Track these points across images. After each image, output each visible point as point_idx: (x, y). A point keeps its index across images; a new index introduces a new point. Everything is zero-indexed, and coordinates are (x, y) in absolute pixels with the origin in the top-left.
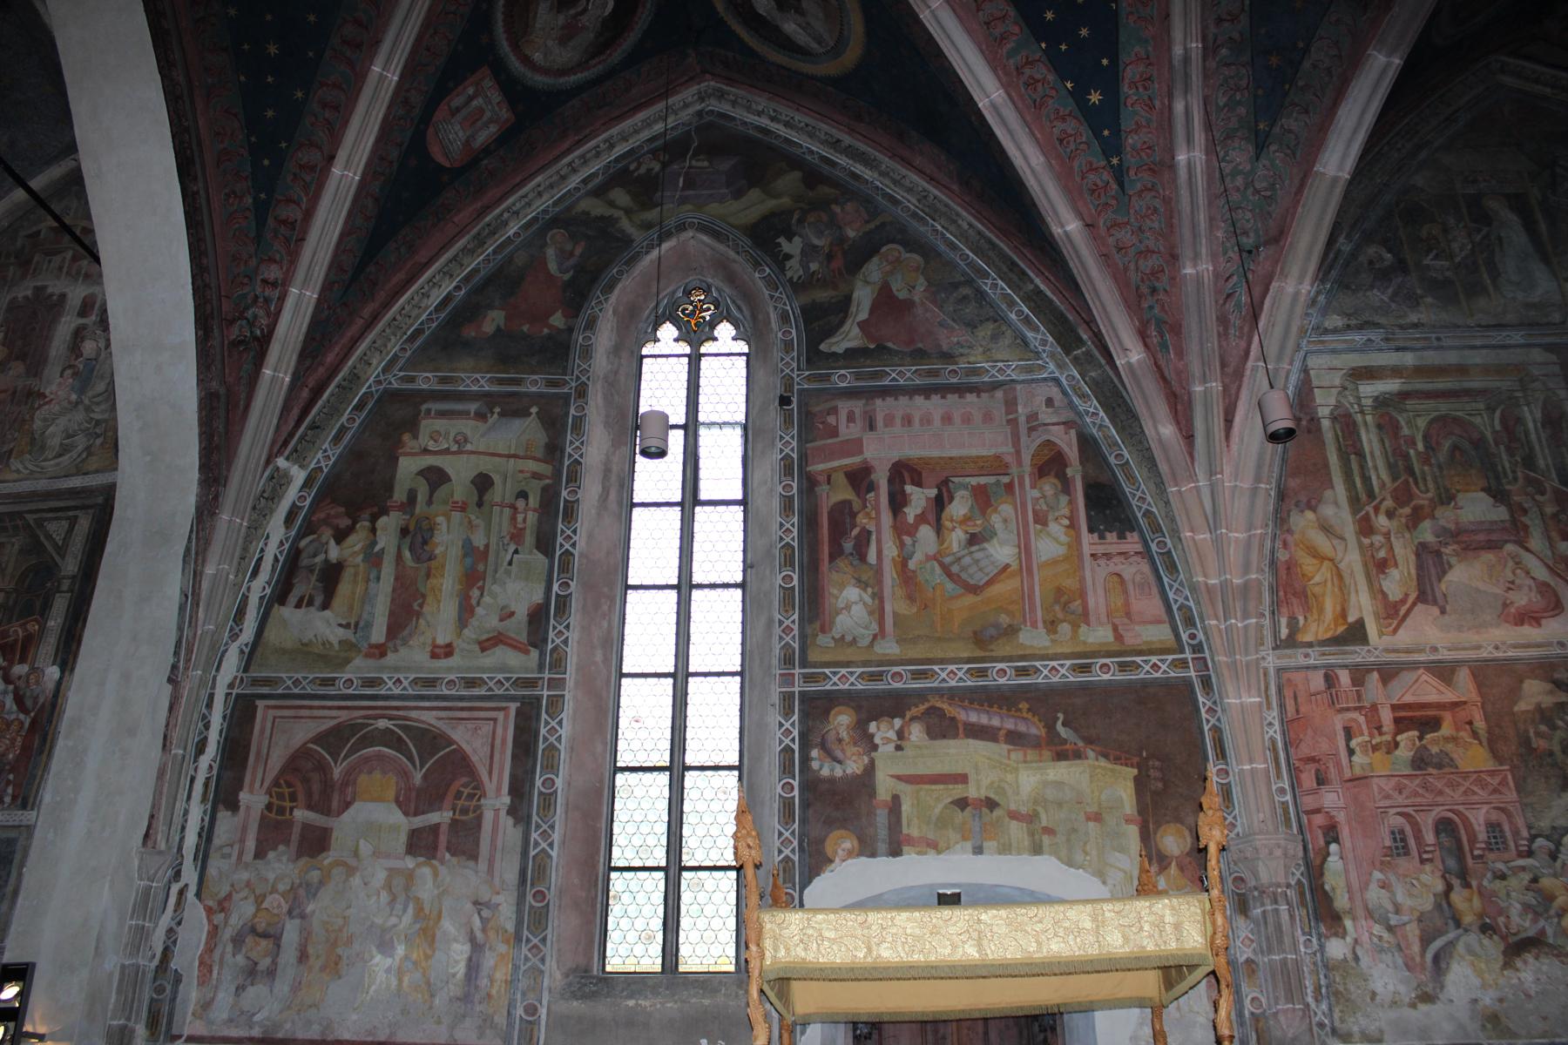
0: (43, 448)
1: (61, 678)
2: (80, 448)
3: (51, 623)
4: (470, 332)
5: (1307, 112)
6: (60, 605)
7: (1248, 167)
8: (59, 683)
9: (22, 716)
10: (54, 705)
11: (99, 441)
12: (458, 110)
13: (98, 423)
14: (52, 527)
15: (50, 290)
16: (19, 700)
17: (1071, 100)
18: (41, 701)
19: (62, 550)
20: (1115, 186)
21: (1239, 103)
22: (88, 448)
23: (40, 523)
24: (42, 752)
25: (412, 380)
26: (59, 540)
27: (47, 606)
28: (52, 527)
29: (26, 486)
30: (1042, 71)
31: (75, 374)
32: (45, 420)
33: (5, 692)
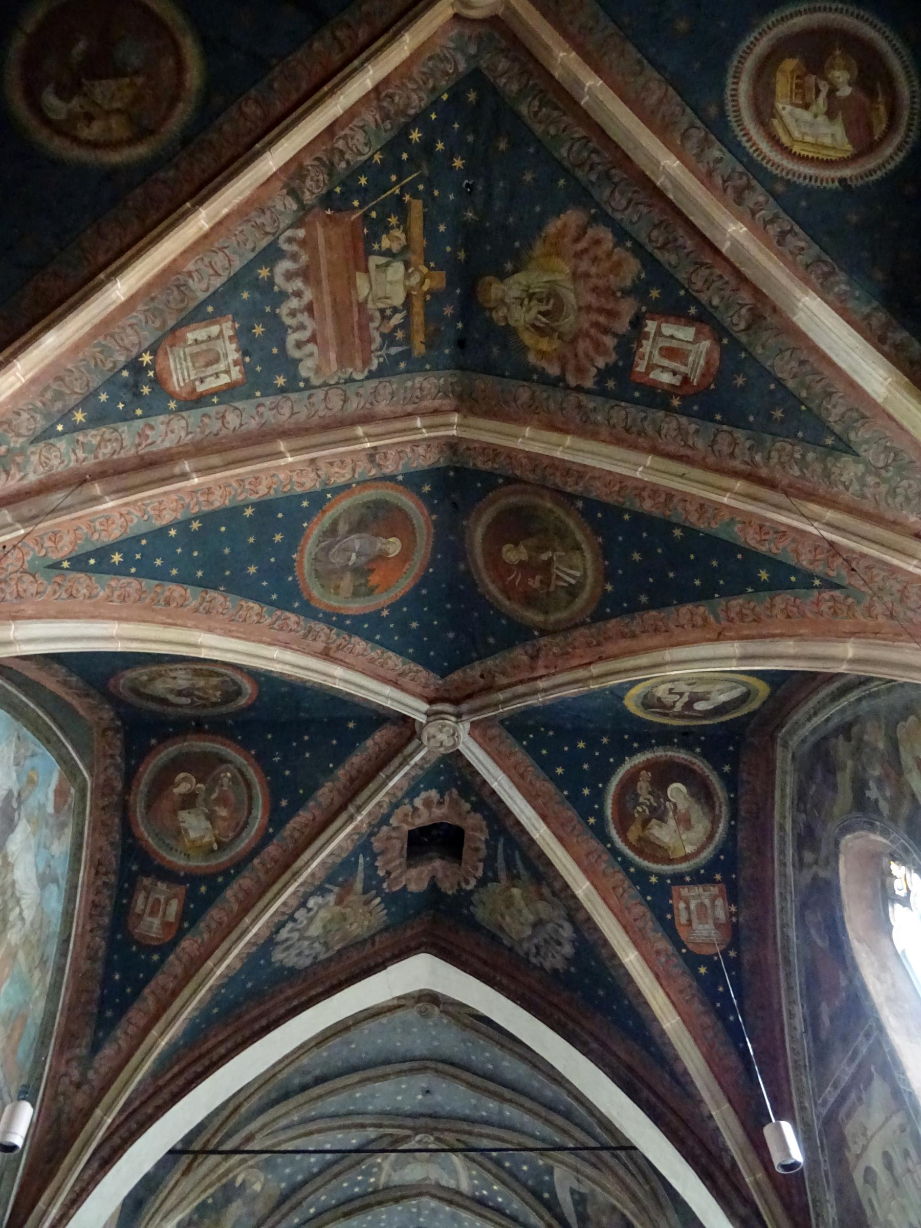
4: (823, 1035)
5: (830, 395)
7: (861, 467)
12: (690, 921)
17: (762, 594)
20: (837, 593)
21: (803, 456)
25: (825, 1102)
30: (736, 603)
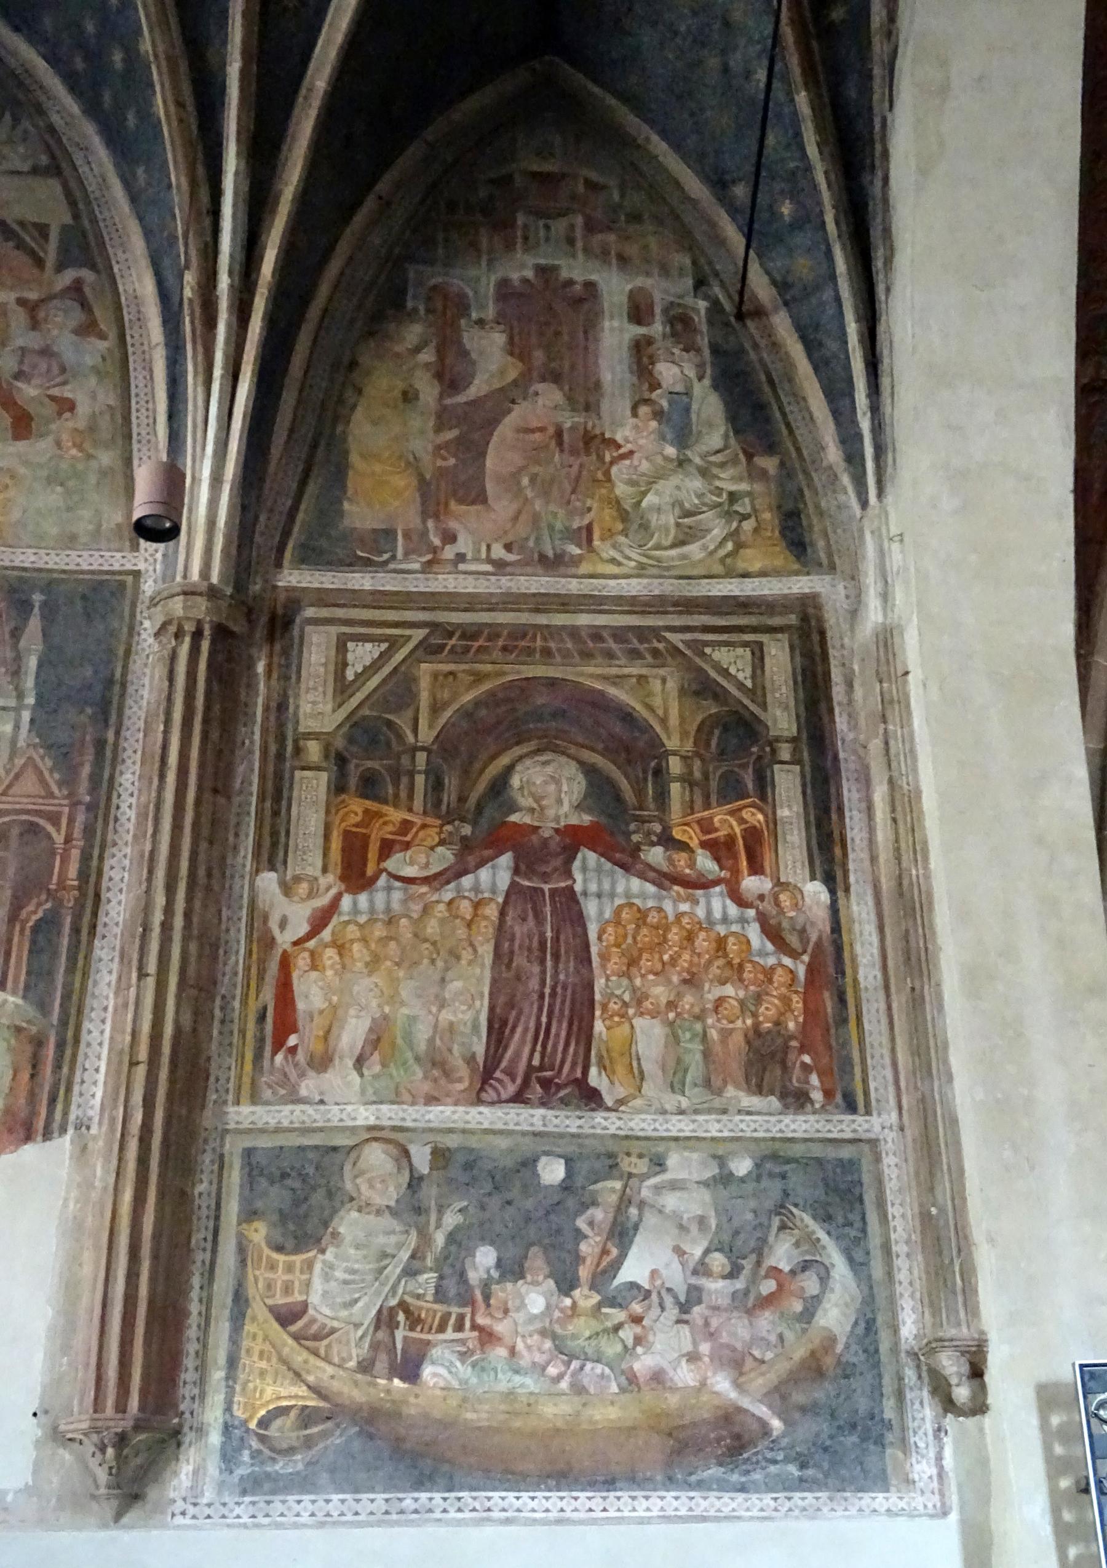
0: (645, 526)
1: (834, 902)
2: (718, 531)
3: (783, 813)
6: (788, 783)
8: (834, 909)
9: (787, 961)
10: (839, 949)
11: (748, 525)
13: (733, 497)
14: (721, 655)
15: (564, 274)
16: (772, 932)
18: (814, 938)
19: (758, 692)
22: (734, 535)
23: (698, 648)
24: (845, 1021)
26: (744, 676)
27: (764, 786)
28: (721, 655)
29: (634, 587)
31: (658, 415)
32: (632, 483)
33: (743, 921)
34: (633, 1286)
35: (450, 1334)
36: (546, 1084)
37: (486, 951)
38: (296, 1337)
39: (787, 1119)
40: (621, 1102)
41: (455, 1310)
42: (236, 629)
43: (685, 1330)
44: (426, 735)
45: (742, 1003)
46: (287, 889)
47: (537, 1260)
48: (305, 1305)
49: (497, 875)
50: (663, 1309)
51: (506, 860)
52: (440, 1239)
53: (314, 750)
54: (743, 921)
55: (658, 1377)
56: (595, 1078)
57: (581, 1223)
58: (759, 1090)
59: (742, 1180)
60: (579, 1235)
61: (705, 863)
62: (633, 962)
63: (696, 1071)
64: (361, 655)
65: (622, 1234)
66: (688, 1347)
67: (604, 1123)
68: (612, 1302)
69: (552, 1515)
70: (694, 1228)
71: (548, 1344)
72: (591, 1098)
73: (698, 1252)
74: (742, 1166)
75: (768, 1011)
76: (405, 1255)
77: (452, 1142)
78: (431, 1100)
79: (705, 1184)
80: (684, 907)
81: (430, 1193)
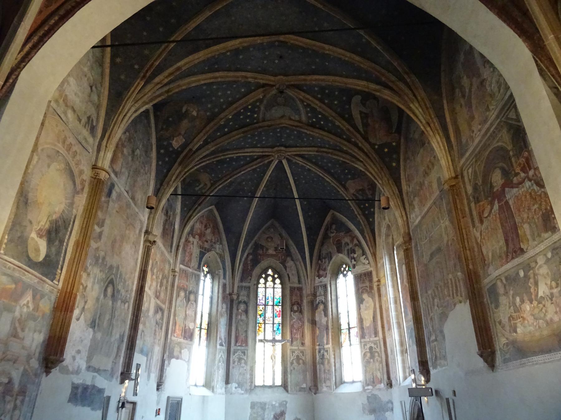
33: (532, 185)
34: (541, 297)
35: (519, 320)
36: (515, 252)
37: (499, 225)
38: (502, 327)
39: (553, 236)
40: (527, 249)
41: (517, 314)
42: (454, 184)
43: (553, 305)
44: (481, 182)
45: (538, 208)
46: (476, 230)
47: (525, 298)
48: (501, 320)
49: (496, 206)
50: (547, 301)
51: (496, 202)
52: (511, 298)
53: (471, 198)
54: (532, 185)
55: (551, 320)
56: (522, 246)
57: (530, 284)
58: (546, 231)
59: (551, 259)
60: (530, 287)
61: (523, 175)
62: (519, 211)
63: (536, 234)
64: (470, 171)
65: (536, 284)
66: (555, 311)
67: (526, 256)
68: (539, 303)
69: (543, 361)
70: (547, 276)
71: (533, 318)
72: (522, 251)
73: (549, 283)
74: (549, 255)
75: (543, 207)
76: (508, 304)
77: (506, 274)
78: (502, 266)
79: (545, 264)
80: (523, 190)
81: (507, 287)
